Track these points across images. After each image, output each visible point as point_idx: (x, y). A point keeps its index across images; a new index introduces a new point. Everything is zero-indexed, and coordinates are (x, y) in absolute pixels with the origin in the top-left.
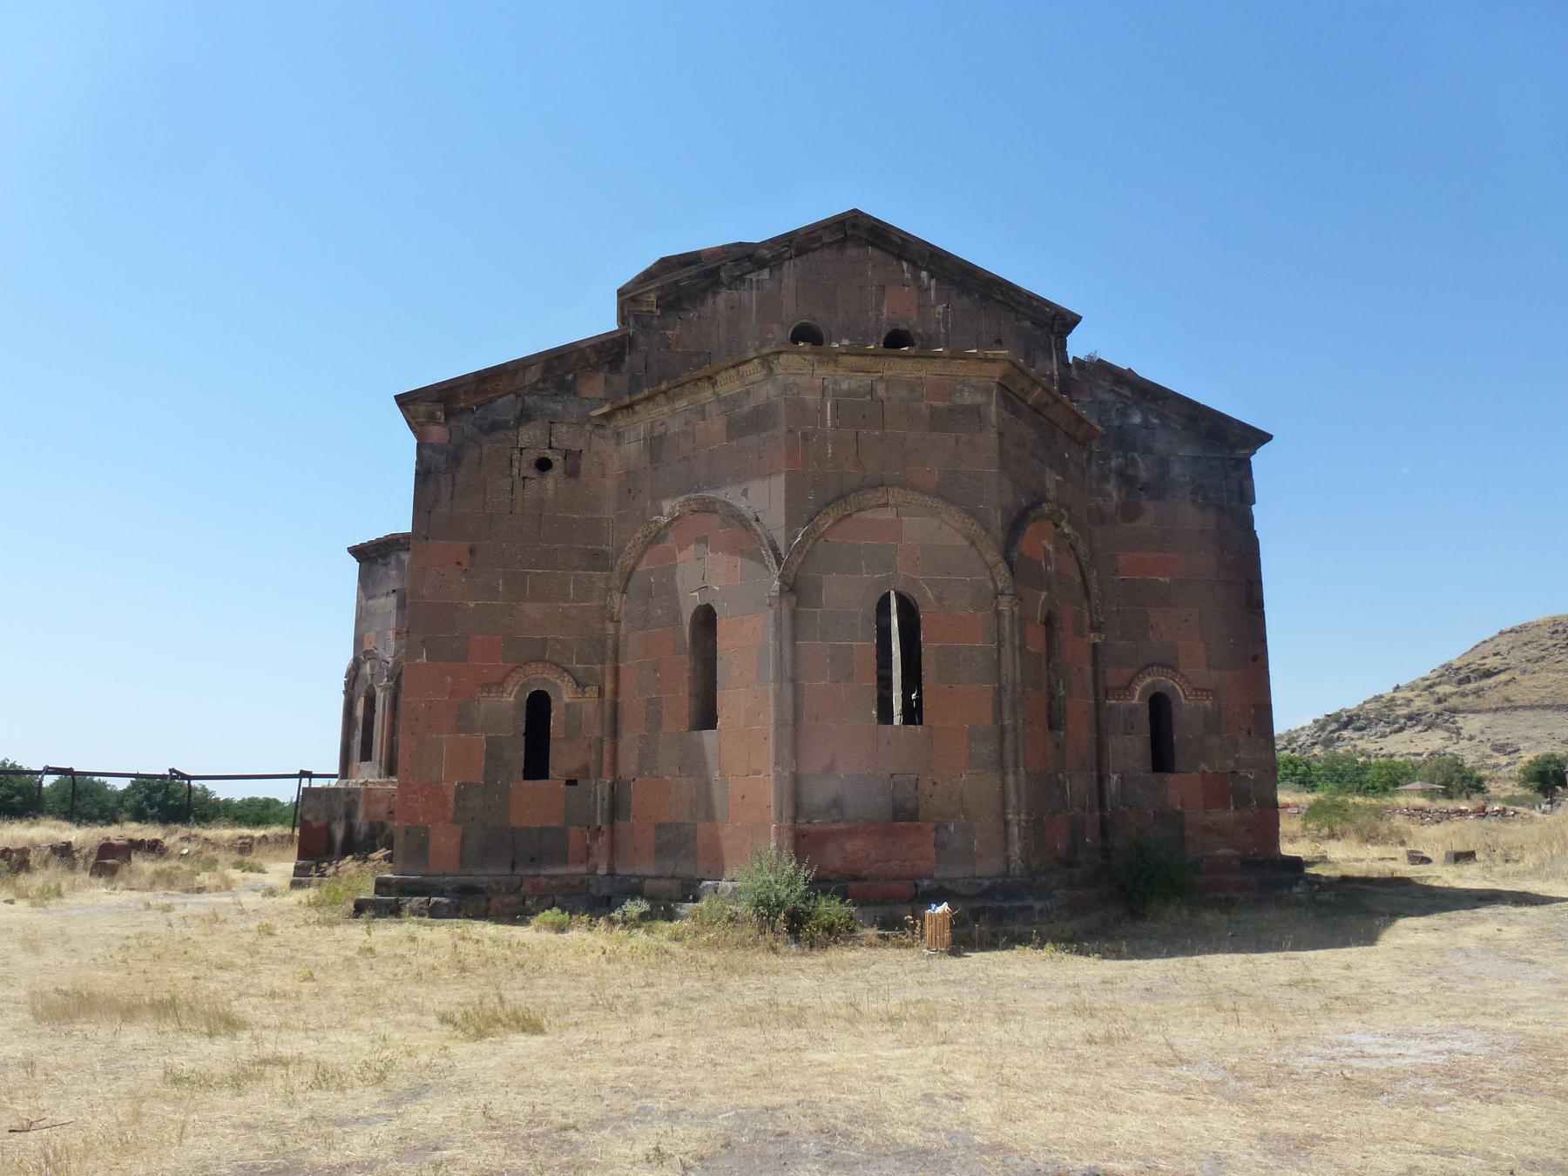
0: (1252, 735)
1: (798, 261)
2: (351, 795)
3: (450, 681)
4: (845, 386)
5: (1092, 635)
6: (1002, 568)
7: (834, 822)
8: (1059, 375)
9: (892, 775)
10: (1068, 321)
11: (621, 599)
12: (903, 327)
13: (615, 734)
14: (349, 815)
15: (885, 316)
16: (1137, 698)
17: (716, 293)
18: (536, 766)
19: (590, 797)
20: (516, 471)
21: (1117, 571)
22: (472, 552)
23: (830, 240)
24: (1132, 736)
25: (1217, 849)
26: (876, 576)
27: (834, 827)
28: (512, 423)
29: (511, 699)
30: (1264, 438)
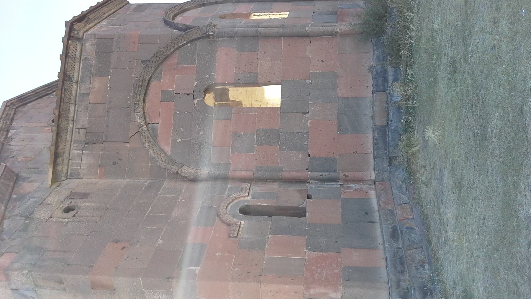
3: (220, 254)
22: (117, 241)
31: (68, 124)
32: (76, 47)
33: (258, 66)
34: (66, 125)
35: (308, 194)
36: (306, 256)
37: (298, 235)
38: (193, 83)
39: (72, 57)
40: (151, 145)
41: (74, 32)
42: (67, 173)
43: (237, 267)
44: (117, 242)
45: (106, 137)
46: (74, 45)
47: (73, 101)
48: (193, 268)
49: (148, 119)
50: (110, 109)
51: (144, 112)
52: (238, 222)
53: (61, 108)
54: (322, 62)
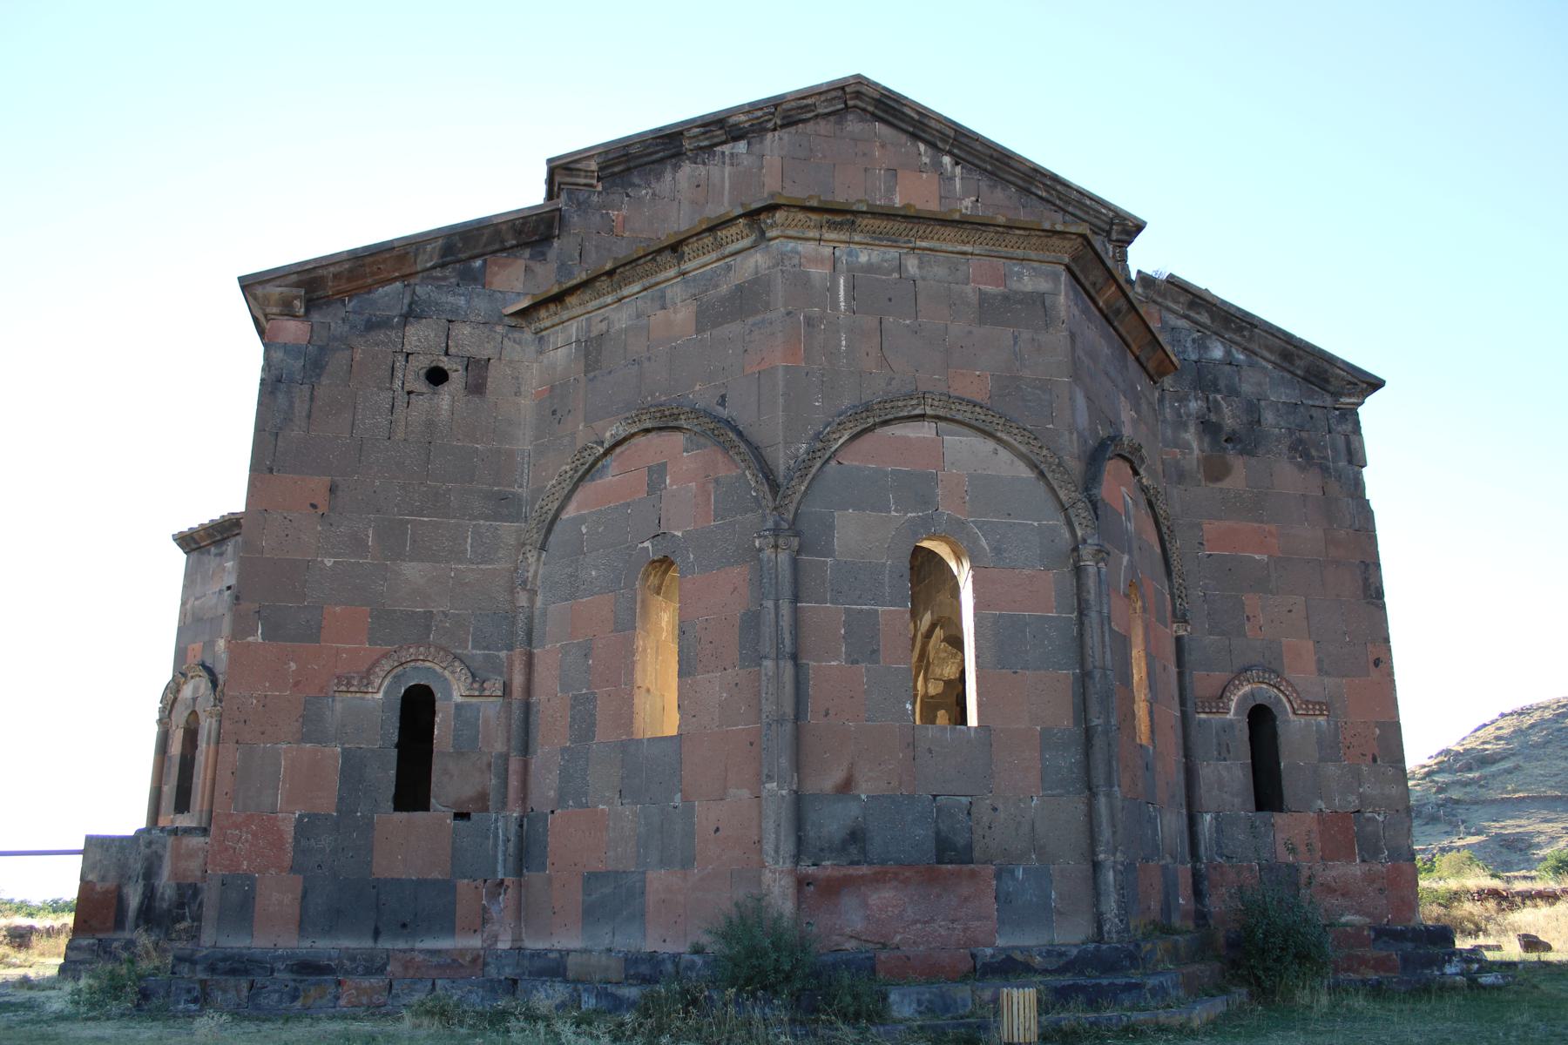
0: (1379, 762)
1: (785, 134)
2: (154, 847)
4: (863, 258)
5: (1175, 625)
6: (1082, 512)
7: (852, 863)
9: (935, 796)
10: (1131, 228)
11: (538, 560)
13: (525, 749)
14: (150, 874)
16: (1234, 712)
17: (676, 167)
19: (488, 838)
20: (398, 383)
21: (1202, 544)
23: (826, 111)
24: (1228, 762)
26: (909, 515)
27: (851, 871)
28: (396, 320)
29: (381, 696)
30: (1375, 384)
31: (608, 293)
32: (742, 238)
33: (708, 672)
34: (605, 291)
36: (284, 814)
37: (341, 799)
38: (678, 529)
39: (719, 239)
40: (568, 475)
41: (768, 218)
42: (542, 330)
43: (258, 701)
44: (330, 490)
45: (595, 377)
46: (742, 231)
47: (647, 282)
48: (260, 631)
49: (618, 450)
50: (638, 364)
51: (625, 440)
53: (621, 269)
54: (715, 828)
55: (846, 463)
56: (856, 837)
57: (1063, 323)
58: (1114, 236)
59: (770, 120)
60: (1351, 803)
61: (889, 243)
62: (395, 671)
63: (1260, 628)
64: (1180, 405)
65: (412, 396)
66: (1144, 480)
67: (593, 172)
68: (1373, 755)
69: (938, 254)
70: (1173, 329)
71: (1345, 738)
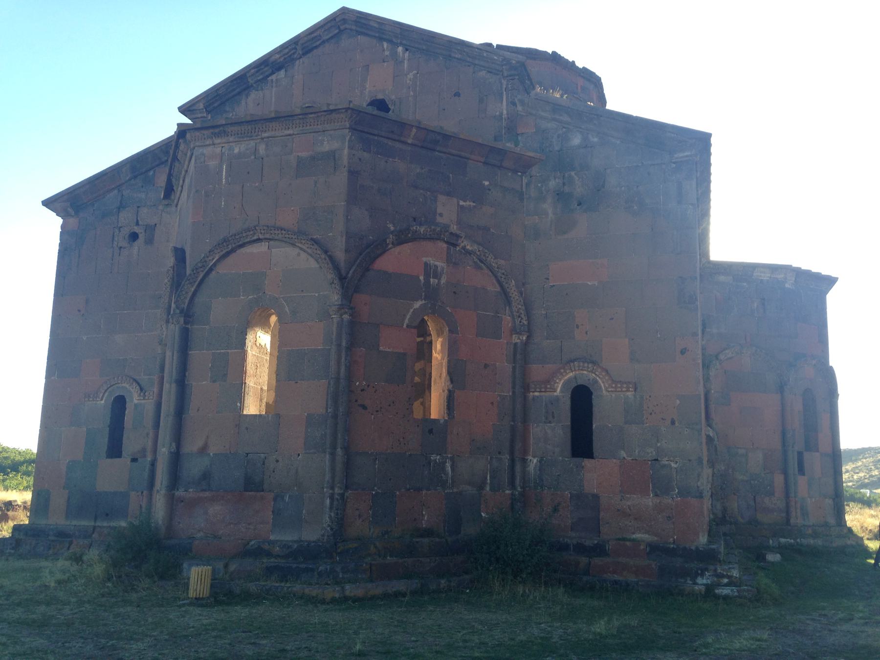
0: (677, 424)
1: (305, 59)
4: (236, 151)
7: (203, 490)
8: (507, 114)
9: (247, 454)
12: (380, 96)
15: (367, 90)
16: (560, 389)
18: (115, 450)
21: (548, 279)
23: (327, 37)
24: (552, 425)
25: (634, 533)
27: (202, 494)
29: (103, 403)
35: (139, 459)
52: (99, 398)
55: (220, 272)
56: (206, 476)
57: (344, 168)
58: (506, 74)
59: (294, 53)
60: (648, 453)
61: (248, 139)
62: (109, 390)
63: (586, 333)
64: (542, 185)
65: (122, 249)
66: (468, 247)
67: (203, 109)
68: (673, 419)
69: (277, 138)
70: (544, 131)
71: (648, 407)
